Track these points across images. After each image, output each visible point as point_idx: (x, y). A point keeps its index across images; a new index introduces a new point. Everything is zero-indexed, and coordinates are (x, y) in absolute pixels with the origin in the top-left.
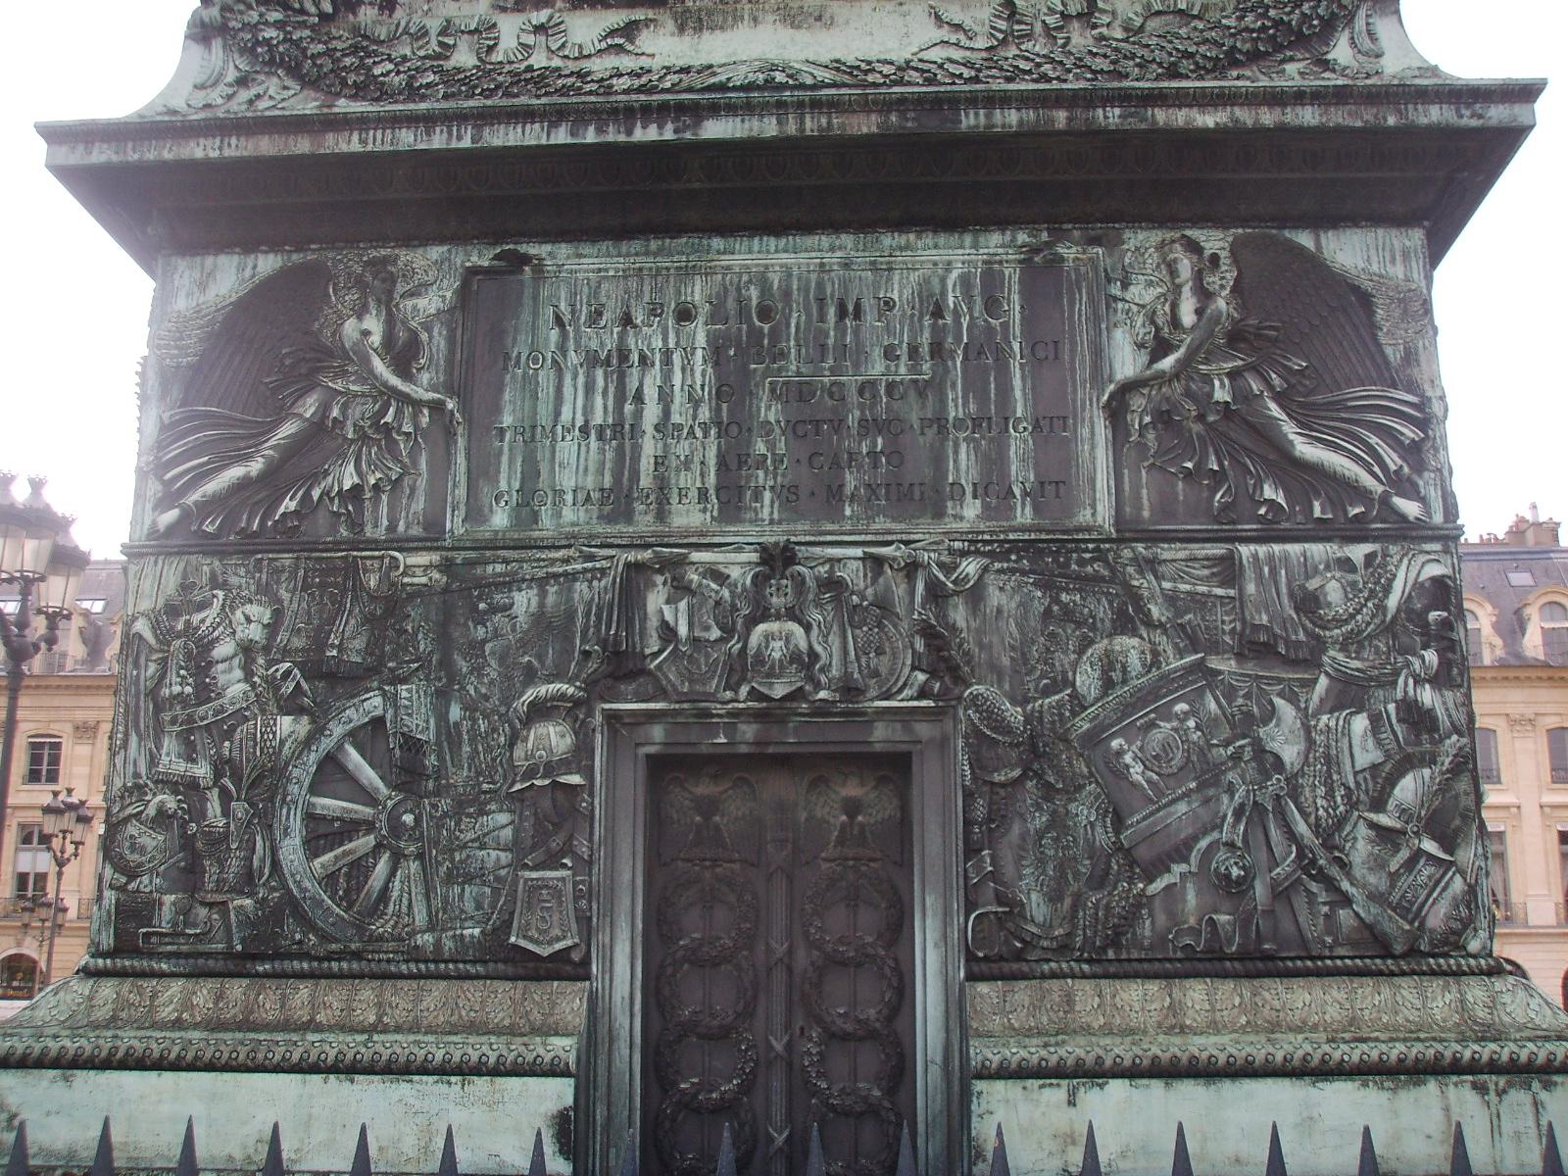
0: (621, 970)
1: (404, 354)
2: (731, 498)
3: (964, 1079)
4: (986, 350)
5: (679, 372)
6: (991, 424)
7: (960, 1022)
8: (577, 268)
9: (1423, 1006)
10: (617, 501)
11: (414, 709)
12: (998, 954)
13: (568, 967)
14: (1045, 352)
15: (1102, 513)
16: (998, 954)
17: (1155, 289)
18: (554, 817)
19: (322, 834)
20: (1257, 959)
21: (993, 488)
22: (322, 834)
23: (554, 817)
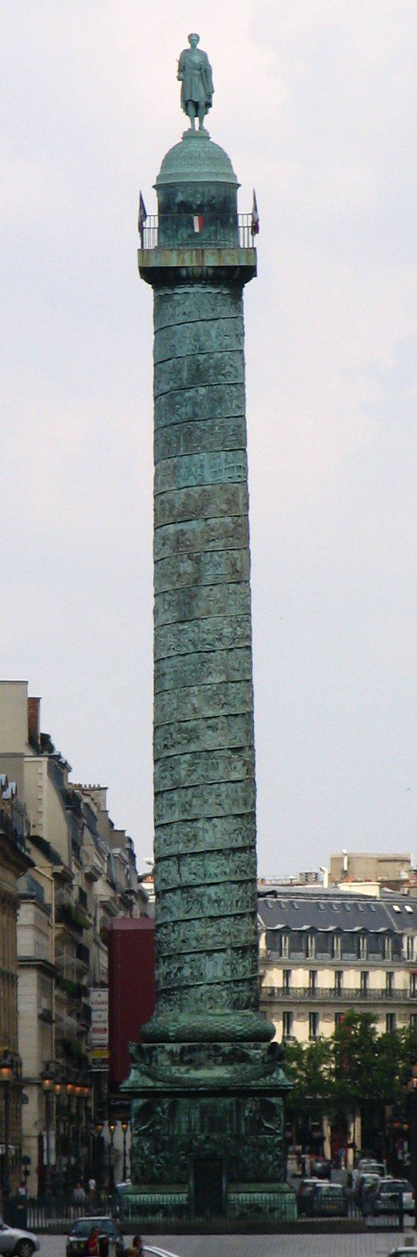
0: (192, 1183)
1: (163, 1112)
2: (202, 1130)
3: (227, 1193)
4: (231, 1112)
5: (196, 1115)
6: (231, 1121)
7: (227, 1187)
8: (184, 1101)
9: (275, 1186)
10: (189, 1130)
11: (167, 1154)
12: (231, 1181)
13: (186, 1183)
14: (238, 1111)
15: (243, 1131)
16: (231, 1181)
17: (250, 1107)
18: (183, 1167)
19: (158, 1168)
20: (258, 1180)
21: (232, 1129)
22: (158, 1168)
23: (183, 1167)
